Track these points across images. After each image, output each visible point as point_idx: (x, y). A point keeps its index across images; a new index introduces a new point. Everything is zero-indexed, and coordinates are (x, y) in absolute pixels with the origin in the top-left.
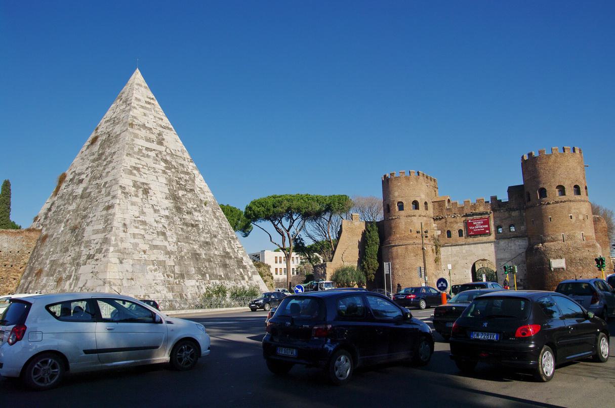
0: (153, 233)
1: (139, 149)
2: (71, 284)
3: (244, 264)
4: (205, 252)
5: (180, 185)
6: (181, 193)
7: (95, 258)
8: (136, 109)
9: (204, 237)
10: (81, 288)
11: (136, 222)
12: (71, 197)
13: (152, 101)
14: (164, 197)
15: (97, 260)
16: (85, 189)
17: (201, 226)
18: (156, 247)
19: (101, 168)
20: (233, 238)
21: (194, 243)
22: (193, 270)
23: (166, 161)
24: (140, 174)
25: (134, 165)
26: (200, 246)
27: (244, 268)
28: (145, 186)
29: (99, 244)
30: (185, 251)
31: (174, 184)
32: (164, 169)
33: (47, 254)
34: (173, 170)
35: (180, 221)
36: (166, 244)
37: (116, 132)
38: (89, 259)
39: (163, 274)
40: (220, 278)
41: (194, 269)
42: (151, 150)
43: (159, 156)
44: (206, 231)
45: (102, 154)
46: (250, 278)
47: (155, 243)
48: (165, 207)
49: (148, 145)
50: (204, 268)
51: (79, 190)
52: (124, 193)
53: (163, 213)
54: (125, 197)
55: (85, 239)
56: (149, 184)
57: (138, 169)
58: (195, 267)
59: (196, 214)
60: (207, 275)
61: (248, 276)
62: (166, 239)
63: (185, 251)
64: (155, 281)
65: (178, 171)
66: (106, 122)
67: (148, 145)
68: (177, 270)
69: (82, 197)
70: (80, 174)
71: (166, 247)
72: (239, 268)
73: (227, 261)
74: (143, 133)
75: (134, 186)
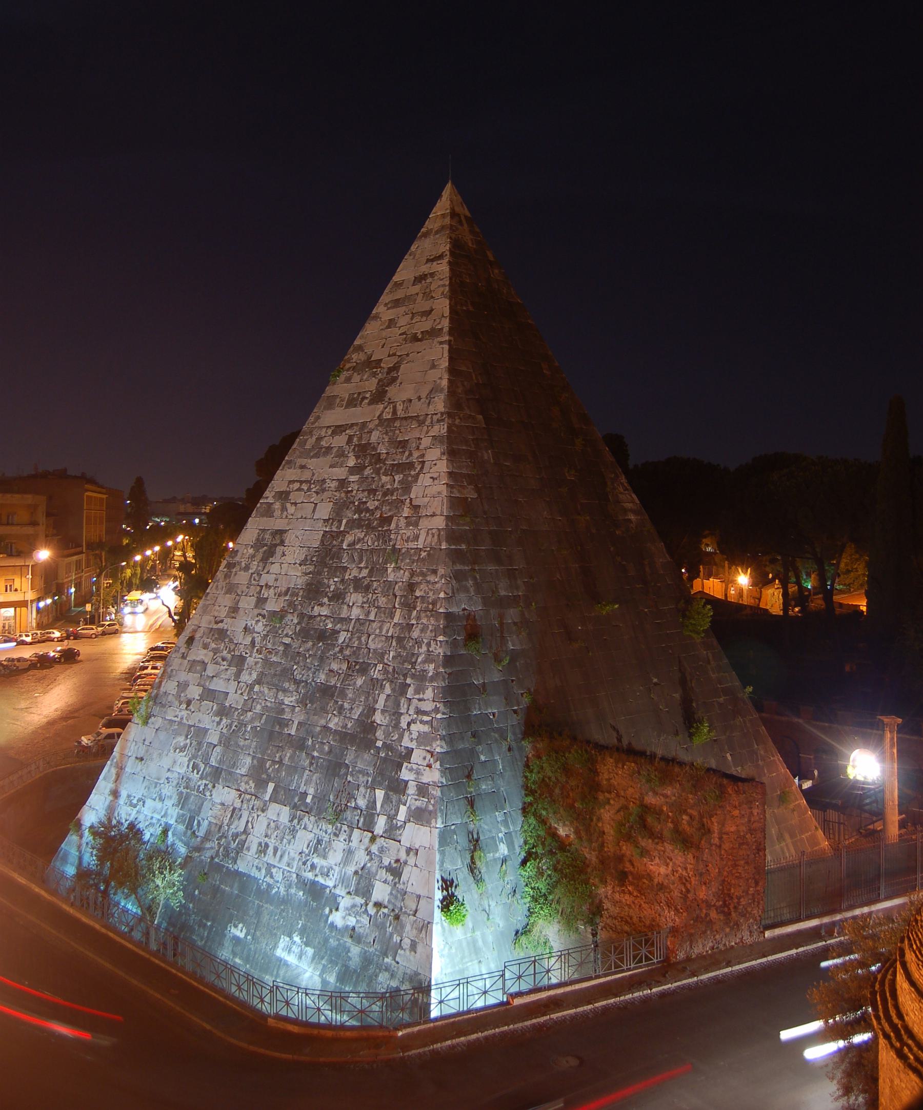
3: (405, 775)
20: (421, 677)
22: (245, 763)
39: (189, 760)
41: (248, 760)
58: (254, 758)
60: (271, 786)
61: (391, 818)
64: (169, 774)
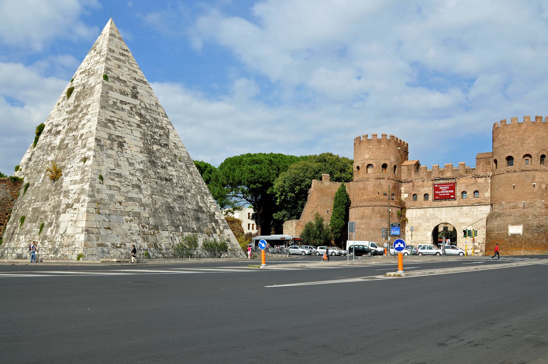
0: (128, 186)
1: (114, 102)
2: (52, 231)
3: (216, 218)
4: (178, 206)
5: (154, 139)
6: (155, 147)
7: (74, 207)
8: (110, 61)
9: (179, 191)
10: (62, 235)
11: (112, 174)
12: (49, 148)
13: (126, 53)
14: (139, 150)
15: (75, 209)
16: (63, 140)
17: (175, 181)
18: (132, 199)
19: (76, 120)
20: (206, 194)
21: (168, 196)
22: (167, 222)
23: (140, 115)
24: (115, 127)
25: (109, 118)
26: (175, 200)
27: (216, 222)
28: (120, 140)
29: (77, 194)
30: (159, 203)
31: (149, 138)
32: (138, 123)
33: (30, 202)
34: (147, 124)
35: (155, 174)
36: (141, 196)
37: (91, 84)
38: (68, 208)
39: (138, 224)
40: (194, 231)
41: (167, 221)
42: (126, 103)
43: (134, 109)
44: (180, 185)
45: (78, 106)
46: (221, 232)
47: (130, 195)
48: (140, 161)
49: (123, 98)
50: (177, 221)
51: (57, 142)
52: (100, 145)
53: (137, 166)
54: (101, 150)
55: (64, 189)
56: (123, 137)
57: (113, 122)
58: (168, 220)
59: (170, 168)
60: (181, 228)
62: (141, 191)
63: (159, 203)
64: (130, 231)
65: (152, 126)
66: (81, 73)
67: (123, 98)
68: (152, 221)
69: (59, 148)
70: (57, 126)
71: (141, 199)
72: (211, 222)
73: (200, 215)
74: (117, 85)
75: (109, 139)
